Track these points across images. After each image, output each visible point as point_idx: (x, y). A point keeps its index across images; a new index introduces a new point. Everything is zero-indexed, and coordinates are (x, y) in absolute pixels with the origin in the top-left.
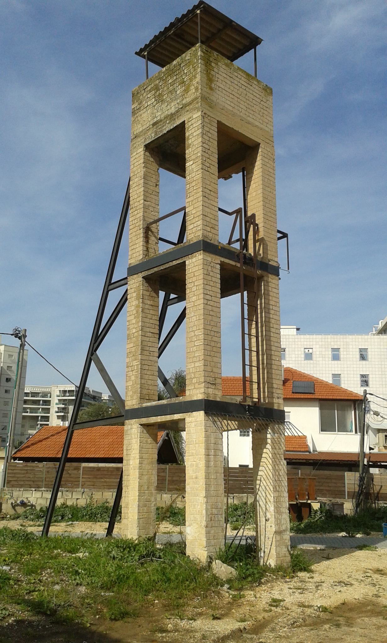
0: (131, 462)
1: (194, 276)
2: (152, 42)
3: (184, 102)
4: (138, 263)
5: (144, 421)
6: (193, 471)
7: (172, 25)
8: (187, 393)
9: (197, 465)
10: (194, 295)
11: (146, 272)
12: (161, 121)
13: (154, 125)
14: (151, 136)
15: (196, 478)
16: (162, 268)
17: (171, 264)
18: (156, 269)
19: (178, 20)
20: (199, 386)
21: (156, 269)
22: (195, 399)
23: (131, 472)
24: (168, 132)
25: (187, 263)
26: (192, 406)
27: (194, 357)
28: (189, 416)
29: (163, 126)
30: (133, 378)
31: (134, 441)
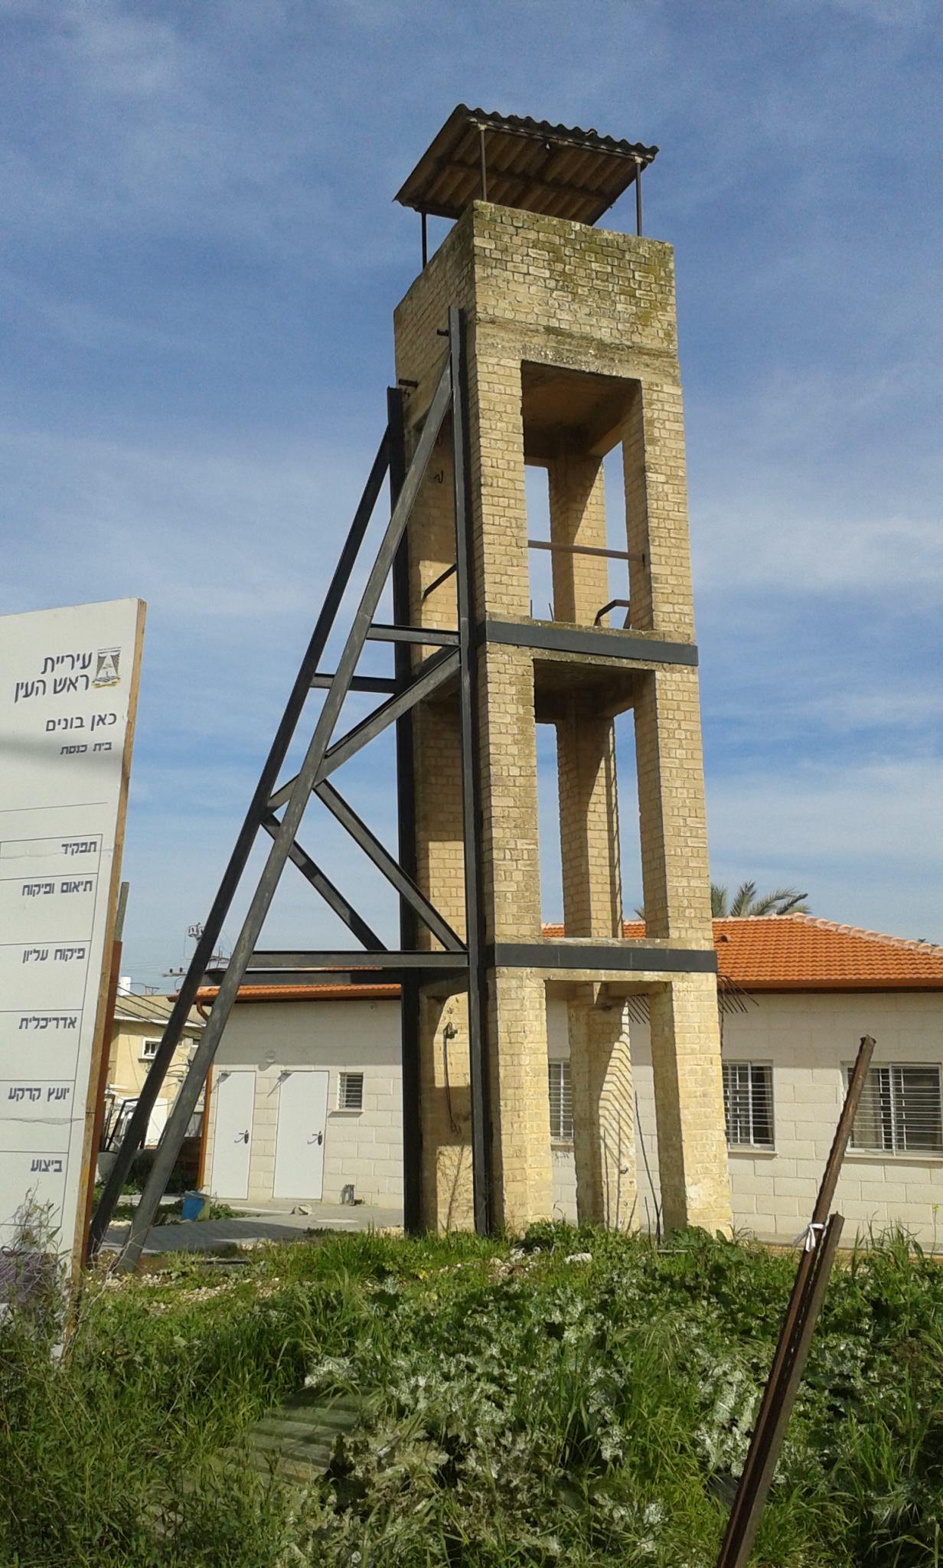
0: (525, 1060)
1: (678, 709)
3: (636, 338)
4: (517, 621)
5: (559, 974)
6: (696, 1082)
7: (577, 132)
8: (674, 933)
9: (705, 1072)
10: (681, 747)
11: (547, 652)
12: (571, 336)
13: (549, 330)
14: (545, 354)
15: (705, 1095)
16: (590, 660)
19: (593, 136)
20: (702, 926)
22: (694, 947)
23: (527, 1081)
24: (590, 373)
26: (690, 961)
28: (683, 980)
29: (580, 353)
30: (518, 876)
31: (530, 1014)
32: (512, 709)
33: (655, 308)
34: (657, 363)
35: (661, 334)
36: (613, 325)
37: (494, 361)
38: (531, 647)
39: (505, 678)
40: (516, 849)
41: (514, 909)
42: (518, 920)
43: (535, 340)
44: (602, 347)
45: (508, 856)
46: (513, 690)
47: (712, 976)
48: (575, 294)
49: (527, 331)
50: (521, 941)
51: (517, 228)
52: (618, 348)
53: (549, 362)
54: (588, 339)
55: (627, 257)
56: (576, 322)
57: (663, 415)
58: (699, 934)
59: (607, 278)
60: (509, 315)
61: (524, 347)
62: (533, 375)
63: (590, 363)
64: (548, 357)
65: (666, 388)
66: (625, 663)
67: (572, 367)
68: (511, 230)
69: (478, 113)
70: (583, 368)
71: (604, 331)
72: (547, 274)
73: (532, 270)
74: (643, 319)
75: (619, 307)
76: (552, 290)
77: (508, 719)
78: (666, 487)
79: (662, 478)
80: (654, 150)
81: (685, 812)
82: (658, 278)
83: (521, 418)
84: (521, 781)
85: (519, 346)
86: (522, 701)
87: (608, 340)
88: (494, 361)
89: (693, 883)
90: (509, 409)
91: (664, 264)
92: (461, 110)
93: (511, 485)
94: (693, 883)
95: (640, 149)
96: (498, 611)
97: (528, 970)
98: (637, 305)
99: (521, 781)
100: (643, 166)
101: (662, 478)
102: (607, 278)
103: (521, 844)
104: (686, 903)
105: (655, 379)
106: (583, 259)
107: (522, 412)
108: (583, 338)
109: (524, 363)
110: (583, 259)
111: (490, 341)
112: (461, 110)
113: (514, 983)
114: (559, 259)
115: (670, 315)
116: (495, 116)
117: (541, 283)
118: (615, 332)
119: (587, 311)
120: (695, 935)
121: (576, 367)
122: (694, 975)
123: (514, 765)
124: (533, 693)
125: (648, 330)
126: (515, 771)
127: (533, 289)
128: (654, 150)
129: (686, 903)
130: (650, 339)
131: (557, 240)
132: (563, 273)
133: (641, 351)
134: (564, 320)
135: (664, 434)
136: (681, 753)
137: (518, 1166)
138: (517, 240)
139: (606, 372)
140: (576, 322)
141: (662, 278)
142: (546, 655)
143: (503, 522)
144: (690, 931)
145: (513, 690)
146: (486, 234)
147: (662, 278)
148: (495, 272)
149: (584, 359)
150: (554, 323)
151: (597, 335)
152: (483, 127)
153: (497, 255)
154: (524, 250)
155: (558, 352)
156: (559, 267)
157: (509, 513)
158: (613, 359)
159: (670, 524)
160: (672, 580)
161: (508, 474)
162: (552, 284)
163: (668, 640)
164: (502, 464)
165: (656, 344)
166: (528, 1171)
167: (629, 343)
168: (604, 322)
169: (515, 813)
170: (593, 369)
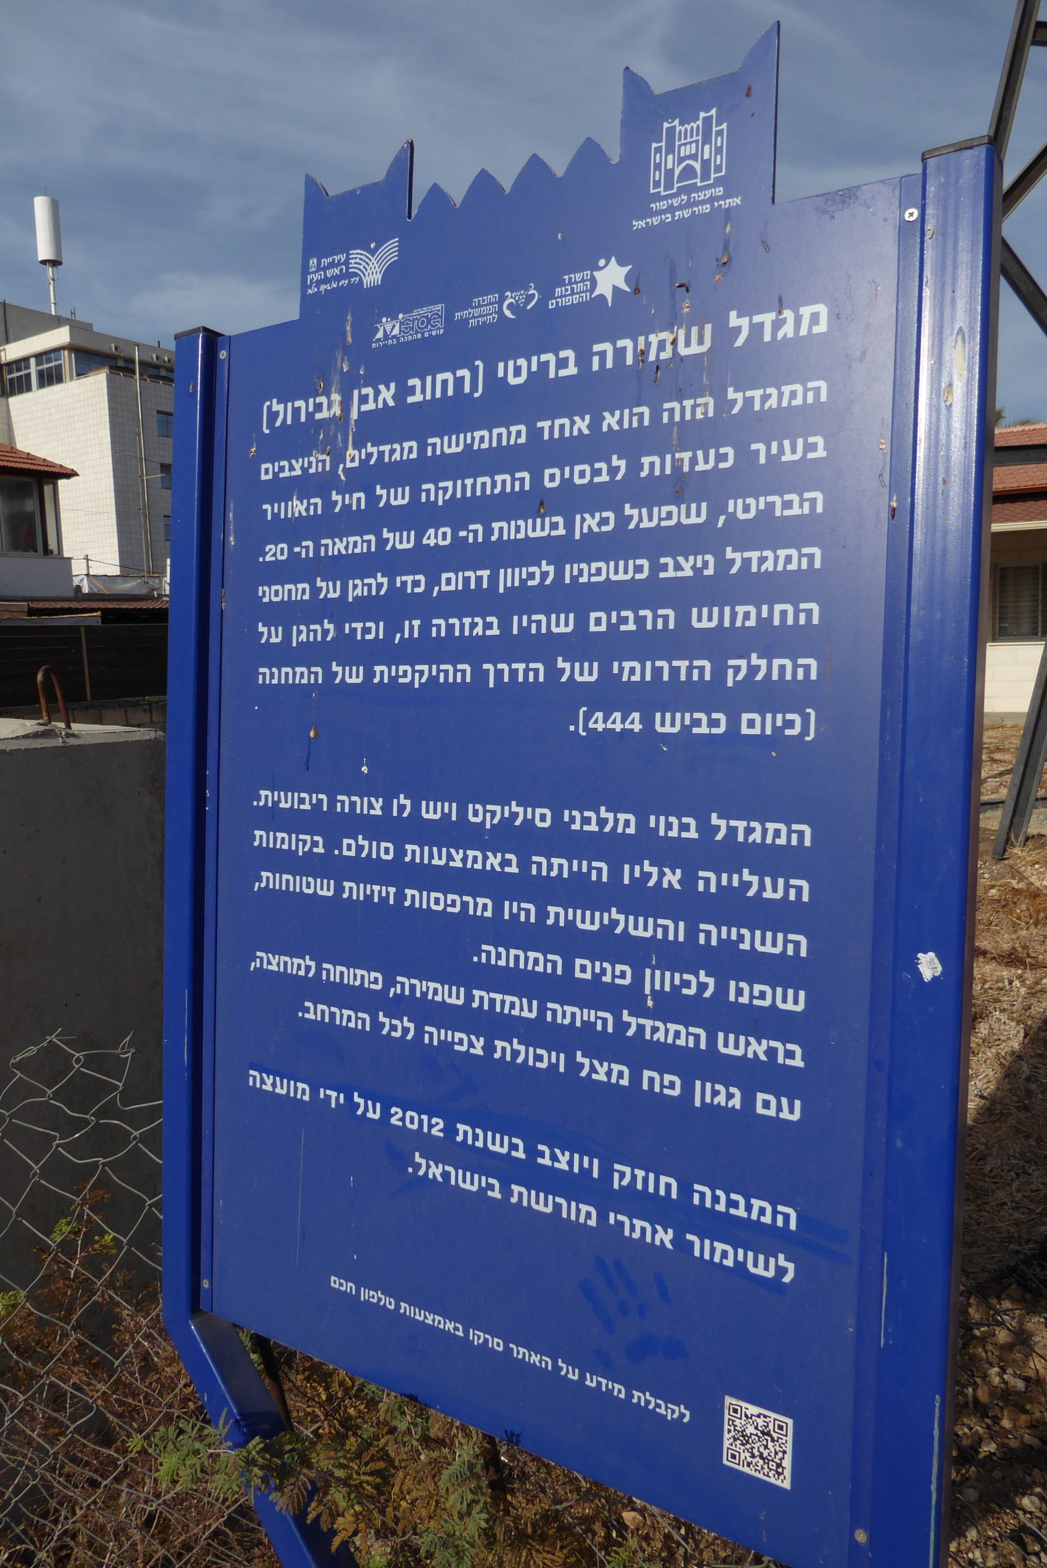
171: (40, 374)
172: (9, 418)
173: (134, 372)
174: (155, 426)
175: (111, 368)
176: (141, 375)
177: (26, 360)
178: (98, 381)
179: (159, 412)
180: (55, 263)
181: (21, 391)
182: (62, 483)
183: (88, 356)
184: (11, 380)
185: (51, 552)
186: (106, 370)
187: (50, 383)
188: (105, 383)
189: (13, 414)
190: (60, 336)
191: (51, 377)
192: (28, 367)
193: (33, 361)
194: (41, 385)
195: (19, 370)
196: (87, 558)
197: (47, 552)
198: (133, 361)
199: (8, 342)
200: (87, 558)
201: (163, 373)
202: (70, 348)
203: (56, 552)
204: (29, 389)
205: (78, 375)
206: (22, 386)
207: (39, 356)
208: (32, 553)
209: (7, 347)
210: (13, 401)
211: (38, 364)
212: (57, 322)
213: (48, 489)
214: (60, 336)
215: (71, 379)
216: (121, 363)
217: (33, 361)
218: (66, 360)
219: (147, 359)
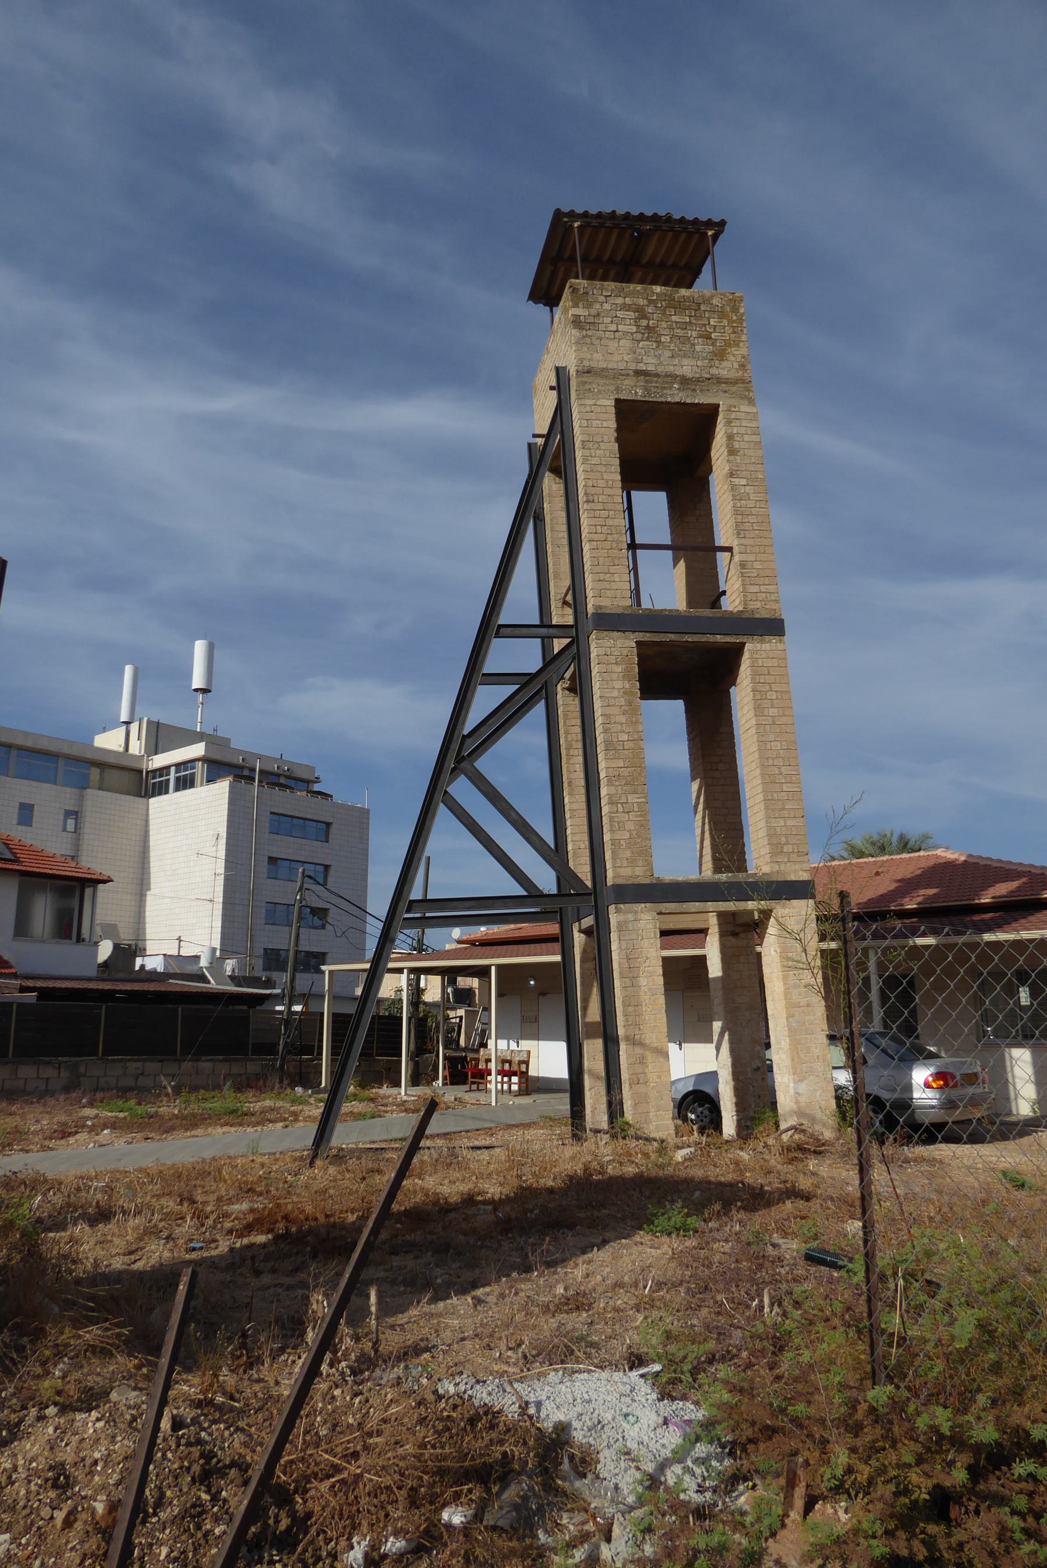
0: (643, 981)
1: (769, 674)
2: (599, 215)
3: (714, 371)
4: (619, 611)
7: (655, 217)
10: (773, 707)
12: (657, 375)
13: (638, 373)
15: (808, 1005)
17: (711, 638)
18: (672, 637)
19: (669, 219)
20: (801, 859)
21: (672, 637)
22: (793, 878)
24: (678, 403)
25: (748, 646)
27: (784, 809)
28: (784, 907)
30: (630, 826)
31: (645, 943)
32: (619, 684)
33: (730, 346)
34: (734, 389)
35: (736, 365)
36: (693, 362)
37: (592, 402)
38: (634, 632)
39: (612, 659)
40: (627, 803)
41: (628, 854)
42: (632, 862)
43: (626, 382)
44: (685, 382)
45: (620, 809)
46: (619, 669)
47: (811, 902)
48: (659, 342)
49: (619, 375)
50: (636, 881)
51: (606, 296)
52: (699, 380)
53: (639, 398)
54: (673, 376)
55: (703, 307)
56: (661, 364)
57: (742, 430)
58: (797, 867)
59: (684, 326)
60: (603, 365)
61: (618, 389)
62: (625, 410)
63: (675, 395)
64: (638, 393)
65: (744, 408)
66: (719, 638)
67: (660, 400)
68: (602, 299)
69: (572, 214)
70: (669, 399)
71: (687, 368)
72: (634, 329)
73: (621, 328)
74: (720, 355)
75: (698, 348)
76: (639, 341)
77: (615, 693)
78: (747, 488)
79: (743, 482)
80: (722, 223)
81: (780, 762)
82: (731, 321)
83: (616, 445)
84: (631, 744)
85: (612, 388)
86: (627, 677)
87: (689, 375)
88: (592, 402)
89: (790, 822)
90: (606, 439)
91: (735, 310)
92: (558, 214)
93: (610, 499)
94: (790, 822)
95: (709, 223)
96: (603, 604)
97: (643, 905)
98: (713, 344)
99: (631, 744)
100: (715, 237)
101: (743, 482)
102: (684, 326)
103: (632, 798)
104: (783, 840)
105: (733, 402)
106: (664, 313)
107: (617, 440)
108: (667, 376)
109: (618, 402)
110: (664, 313)
111: (587, 387)
112: (558, 214)
113: (630, 917)
114: (644, 316)
115: (743, 350)
116: (586, 214)
117: (629, 336)
118: (695, 369)
119: (669, 354)
120: (793, 868)
121: (663, 400)
122: (795, 902)
123: (623, 732)
124: (637, 670)
125: (725, 364)
126: (625, 737)
127: (622, 342)
128: (722, 223)
129: (783, 840)
130: (726, 369)
131: (641, 302)
132: (648, 327)
133: (719, 380)
134: (650, 364)
135: (743, 445)
136: (773, 712)
137: (640, 1071)
138: (607, 306)
139: (689, 401)
140: (661, 364)
141: (734, 321)
142: (647, 637)
143: (605, 530)
144: (788, 864)
145: (619, 669)
146: (581, 305)
147: (734, 321)
148: (589, 333)
149: (669, 392)
150: (642, 367)
151: (679, 372)
152: (576, 225)
153: (591, 319)
154: (613, 313)
155: (646, 389)
156: (644, 322)
157: (610, 522)
158: (694, 390)
159: (751, 519)
160: (757, 565)
161: (607, 491)
162: (639, 336)
163: (758, 616)
164: (601, 483)
165: (733, 375)
166: (649, 1075)
167: (708, 376)
168: (685, 361)
169: (625, 772)
170: (677, 400)
171: (178, 779)
172: (147, 815)
173: (253, 780)
174: (268, 825)
175: (236, 776)
176: (260, 781)
177: (168, 768)
178: (223, 787)
179: (272, 813)
180: (205, 691)
181: (160, 794)
182: (101, 886)
183: (217, 767)
184: (154, 784)
185: (84, 940)
186: (231, 778)
187: (185, 788)
188: (227, 789)
189: (150, 812)
190: (197, 750)
191: (186, 783)
192: (168, 774)
193: (173, 769)
194: (177, 789)
195: (161, 776)
196: (179, 940)
197: (79, 939)
198: (254, 770)
199: (156, 754)
200: (179, 940)
201: (282, 780)
202: (203, 759)
203: (87, 940)
204: (167, 792)
205: (208, 781)
206: (161, 789)
207: (178, 766)
208: (68, 941)
209: (154, 757)
210: (152, 800)
211: (177, 772)
212: (199, 737)
213: (88, 892)
214: (197, 750)
215: (202, 785)
216: (246, 773)
217: (173, 769)
218: (200, 769)
219: (268, 767)
